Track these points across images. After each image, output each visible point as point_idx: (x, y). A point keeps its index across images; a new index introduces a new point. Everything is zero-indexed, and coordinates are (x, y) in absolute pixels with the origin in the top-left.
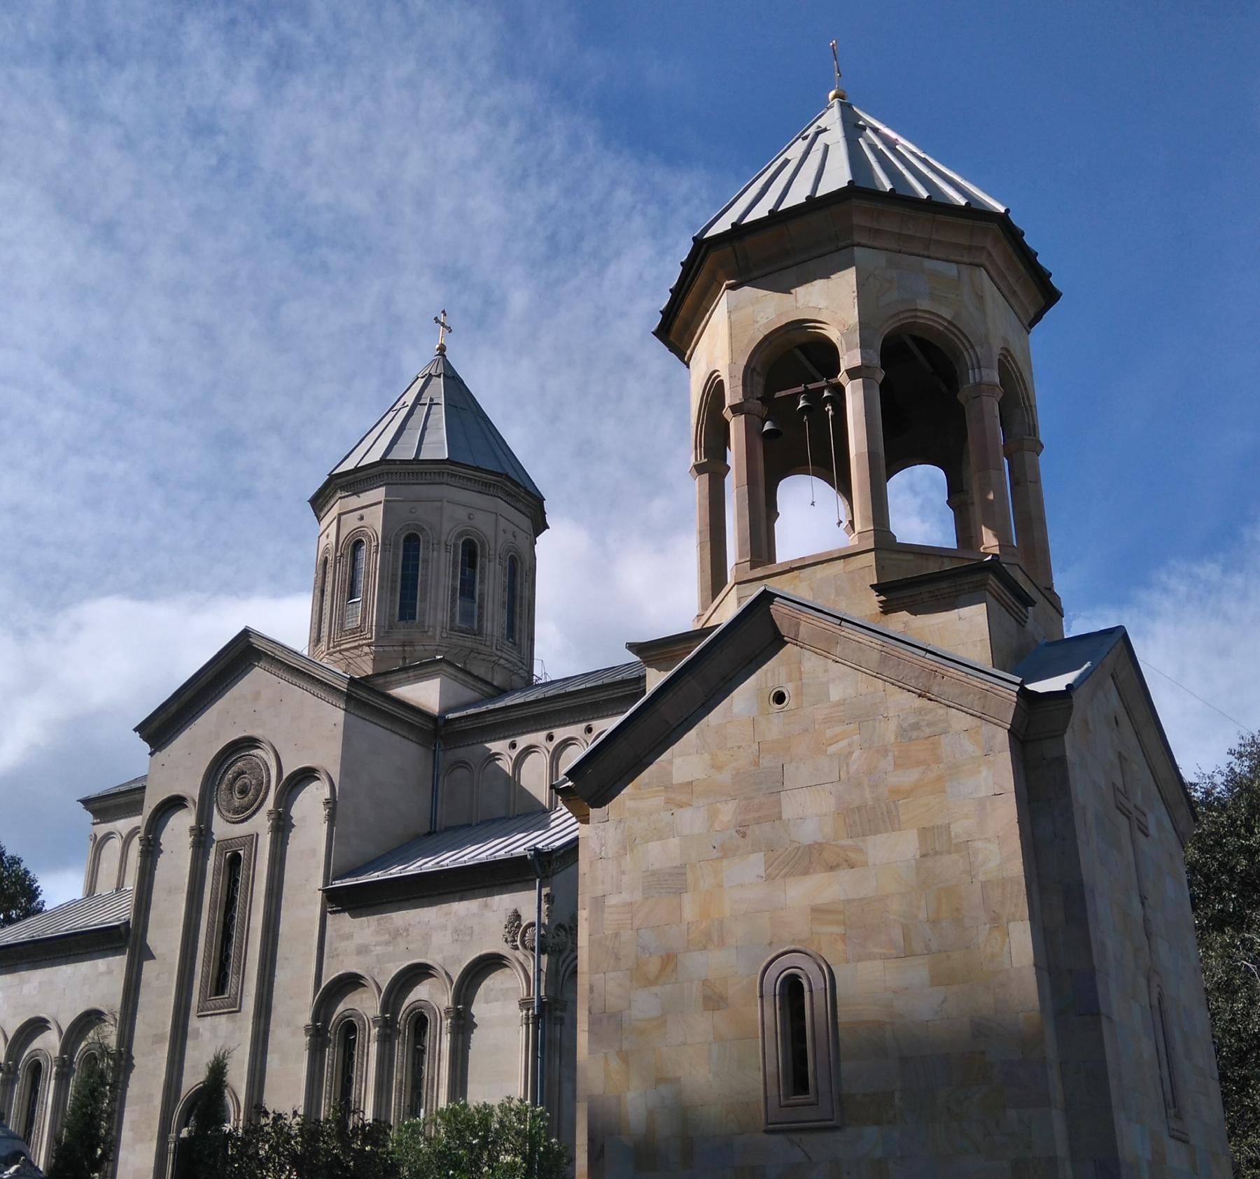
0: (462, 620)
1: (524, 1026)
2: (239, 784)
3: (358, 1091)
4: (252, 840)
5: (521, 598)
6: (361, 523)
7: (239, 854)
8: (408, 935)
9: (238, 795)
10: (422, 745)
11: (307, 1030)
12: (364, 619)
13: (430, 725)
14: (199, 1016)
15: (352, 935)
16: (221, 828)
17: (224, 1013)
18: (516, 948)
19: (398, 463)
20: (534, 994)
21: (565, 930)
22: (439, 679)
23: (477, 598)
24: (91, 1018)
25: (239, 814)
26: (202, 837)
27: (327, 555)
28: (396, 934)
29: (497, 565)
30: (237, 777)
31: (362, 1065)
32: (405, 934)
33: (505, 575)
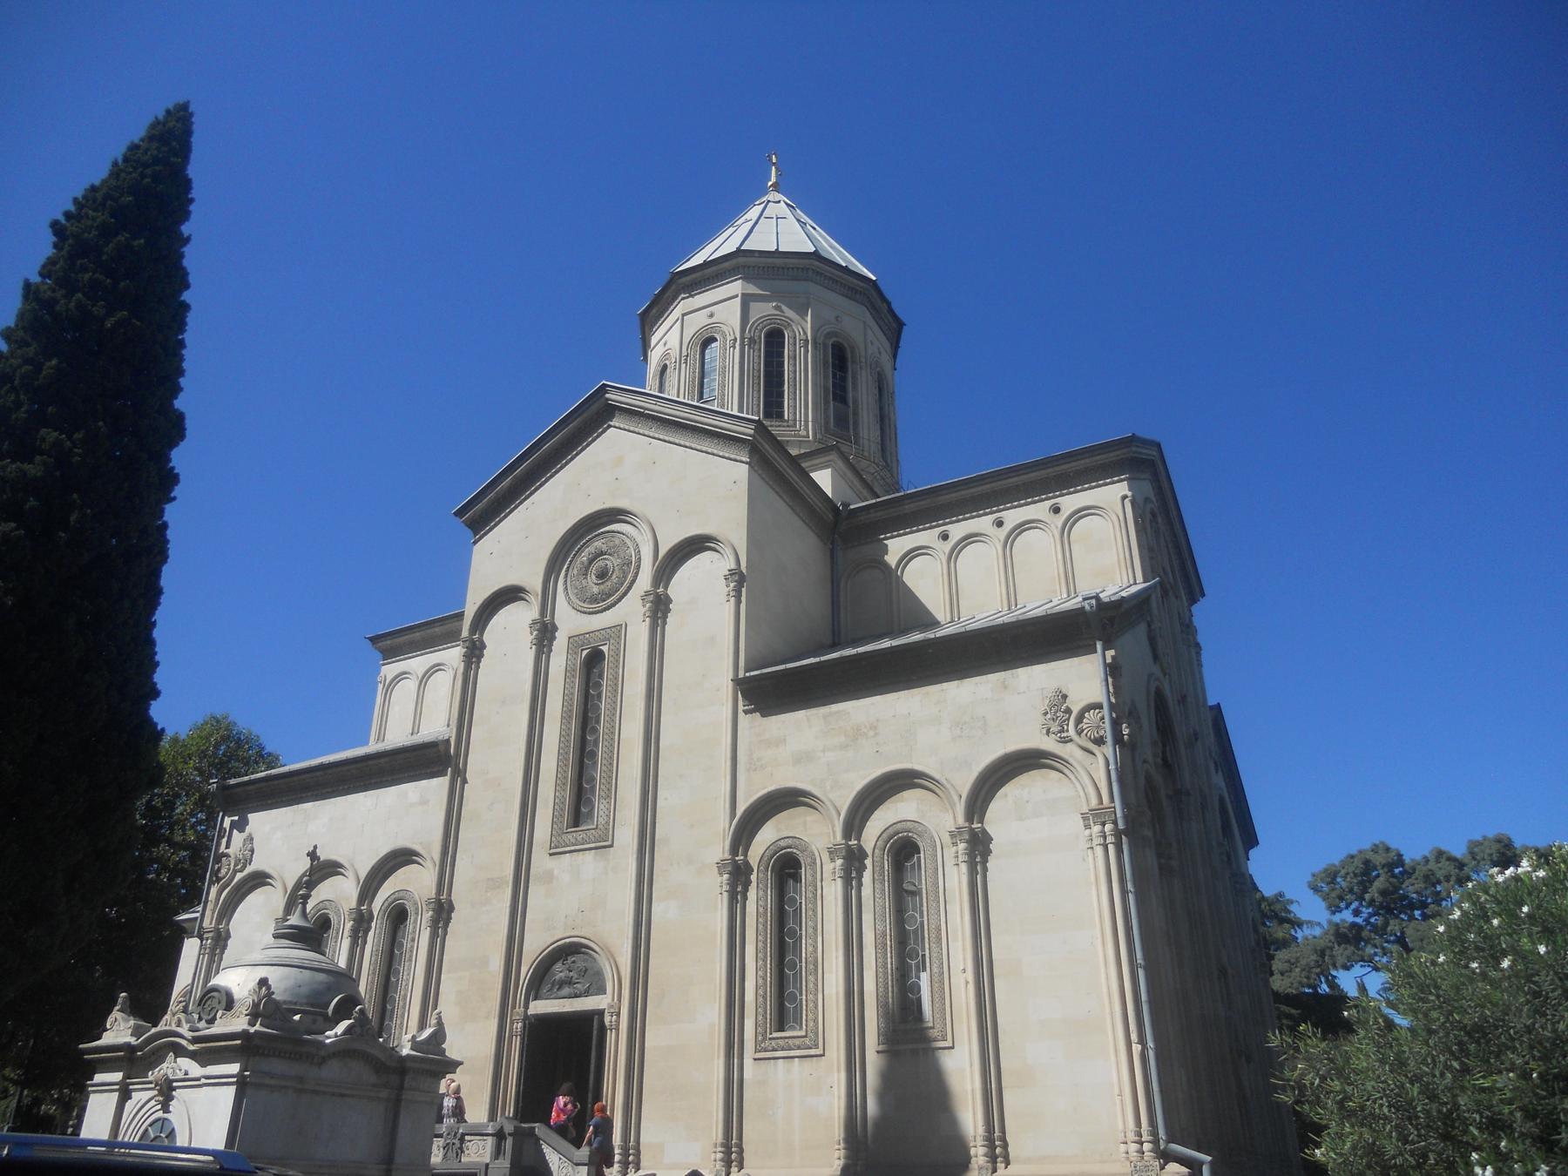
1: (1099, 851)
3: (810, 949)
4: (618, 632)
7: (602, 652)
8: (876, 734)
9: (594, 577)
14: (551, 855)
15: (785, 740)
16: (569, 621)
20: (1112, 799)
22: (830, 470)
23: (851, 405)
24: (401, 858)
25: (598, 603)
26: (545, 633)
27: (667, 362)
28: (857, 734)
30: (593, 560)
31: (815, 911)
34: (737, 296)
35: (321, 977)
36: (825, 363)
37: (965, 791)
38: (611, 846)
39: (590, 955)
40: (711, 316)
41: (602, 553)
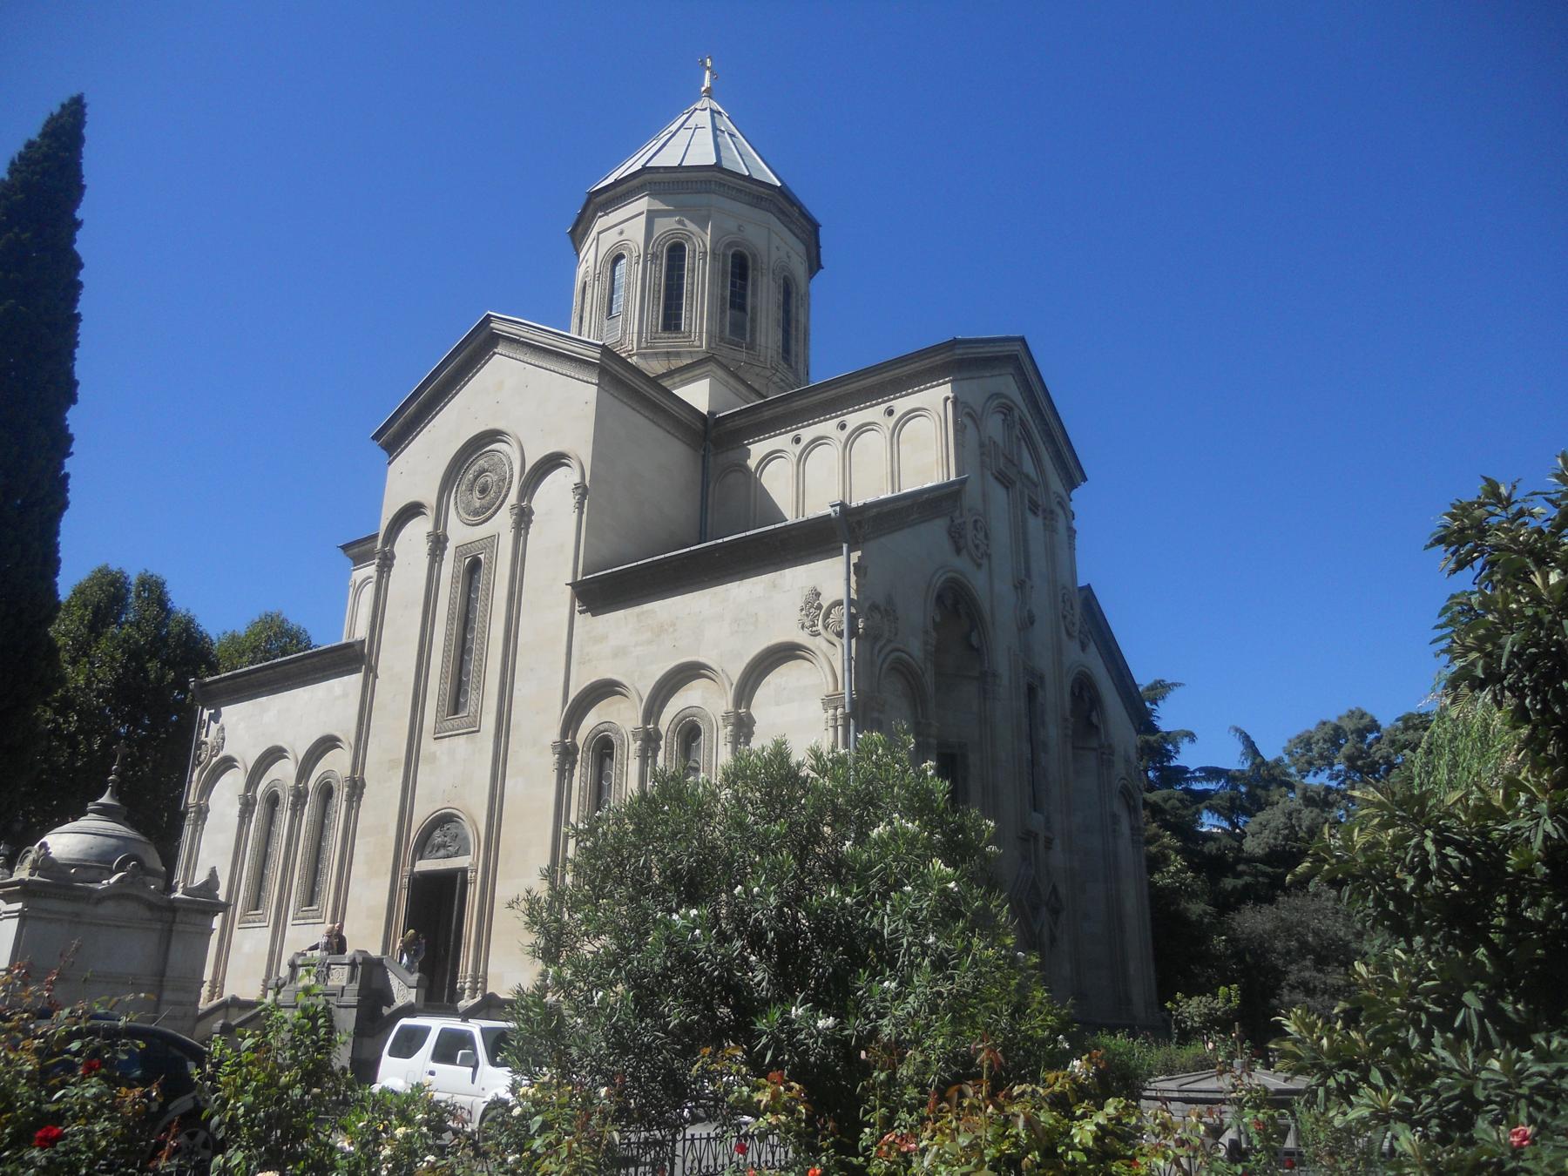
0: (732, 332)
1: (831, 730)
2: (482, 480)
4: (493, 540)
5: (797, 321)
6: (622, 238)
10: (688, 445)
11: (554, 747)
12: (624, 332)
13: (699, 424)
16: (459, 533)
17: (463, 734)
18: (816, 634)
19: (662, 170)
20: (844, 688)
21: (880, 612)
26: (438, 542)
29: (771, 282)
31: (620, 785)
32: (671, 629)
33: (780, 292)
34: (643, 213)
35: (112, 841)
36: (724, 272)
37: (735, 678)
38: (478, 731)
39: (457, 822)
40: (621, 233)
41: (484, 471)
